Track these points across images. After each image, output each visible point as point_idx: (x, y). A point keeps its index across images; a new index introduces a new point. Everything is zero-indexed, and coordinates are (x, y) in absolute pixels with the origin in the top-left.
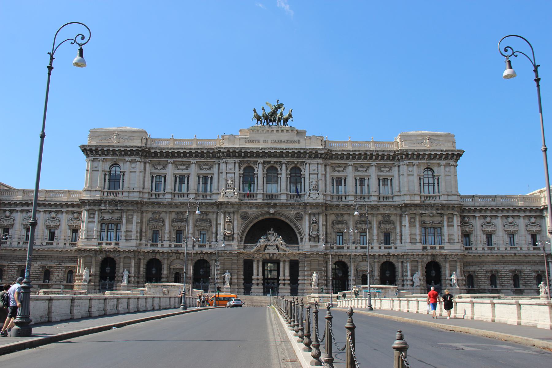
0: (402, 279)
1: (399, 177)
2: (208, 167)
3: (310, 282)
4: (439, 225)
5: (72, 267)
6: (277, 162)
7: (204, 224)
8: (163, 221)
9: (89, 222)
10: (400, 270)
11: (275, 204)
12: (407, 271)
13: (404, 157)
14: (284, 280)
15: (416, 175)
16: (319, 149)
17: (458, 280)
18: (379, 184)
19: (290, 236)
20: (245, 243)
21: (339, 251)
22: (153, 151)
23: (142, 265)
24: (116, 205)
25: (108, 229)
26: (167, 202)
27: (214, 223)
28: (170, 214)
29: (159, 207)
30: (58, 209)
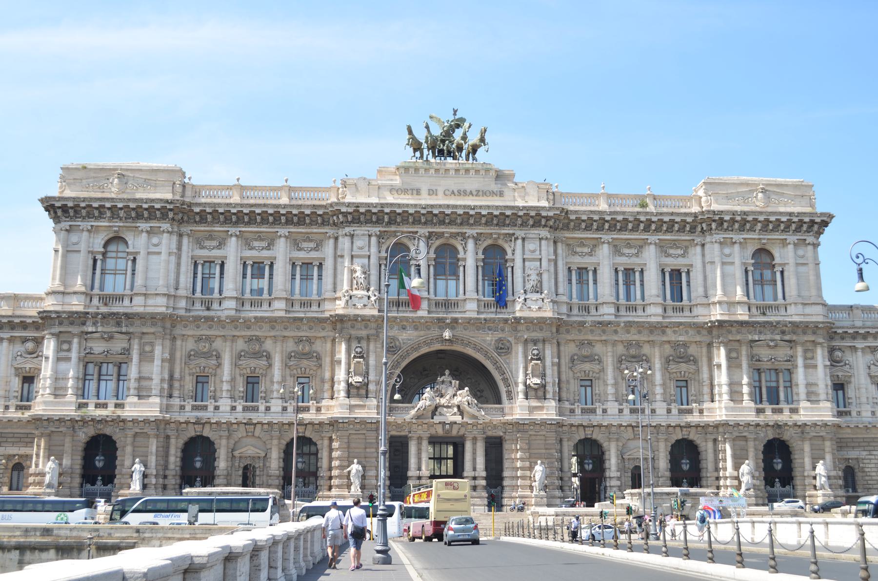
0: (716, 474)
2: (312, 245)
3: (528, 482)
4: (788, 365)
5: (21, 456)
6: (458, 234)
7: (305, 363)
8: (218, 357)
9: (58, 360)
10: (710, 456)
11: (455, 320)
12: (725, 460)
13: (714, 226)
14: (475, 478)
15: (737, 262)
16: (543, 208)
21: (584, 420)
22: (197, 210)
23: (172, 451)
24: (118, 324)
25: (100, 375)
26: (227, 317)
27: (327, 360)
28: (233, 341)
29: (210, 327)
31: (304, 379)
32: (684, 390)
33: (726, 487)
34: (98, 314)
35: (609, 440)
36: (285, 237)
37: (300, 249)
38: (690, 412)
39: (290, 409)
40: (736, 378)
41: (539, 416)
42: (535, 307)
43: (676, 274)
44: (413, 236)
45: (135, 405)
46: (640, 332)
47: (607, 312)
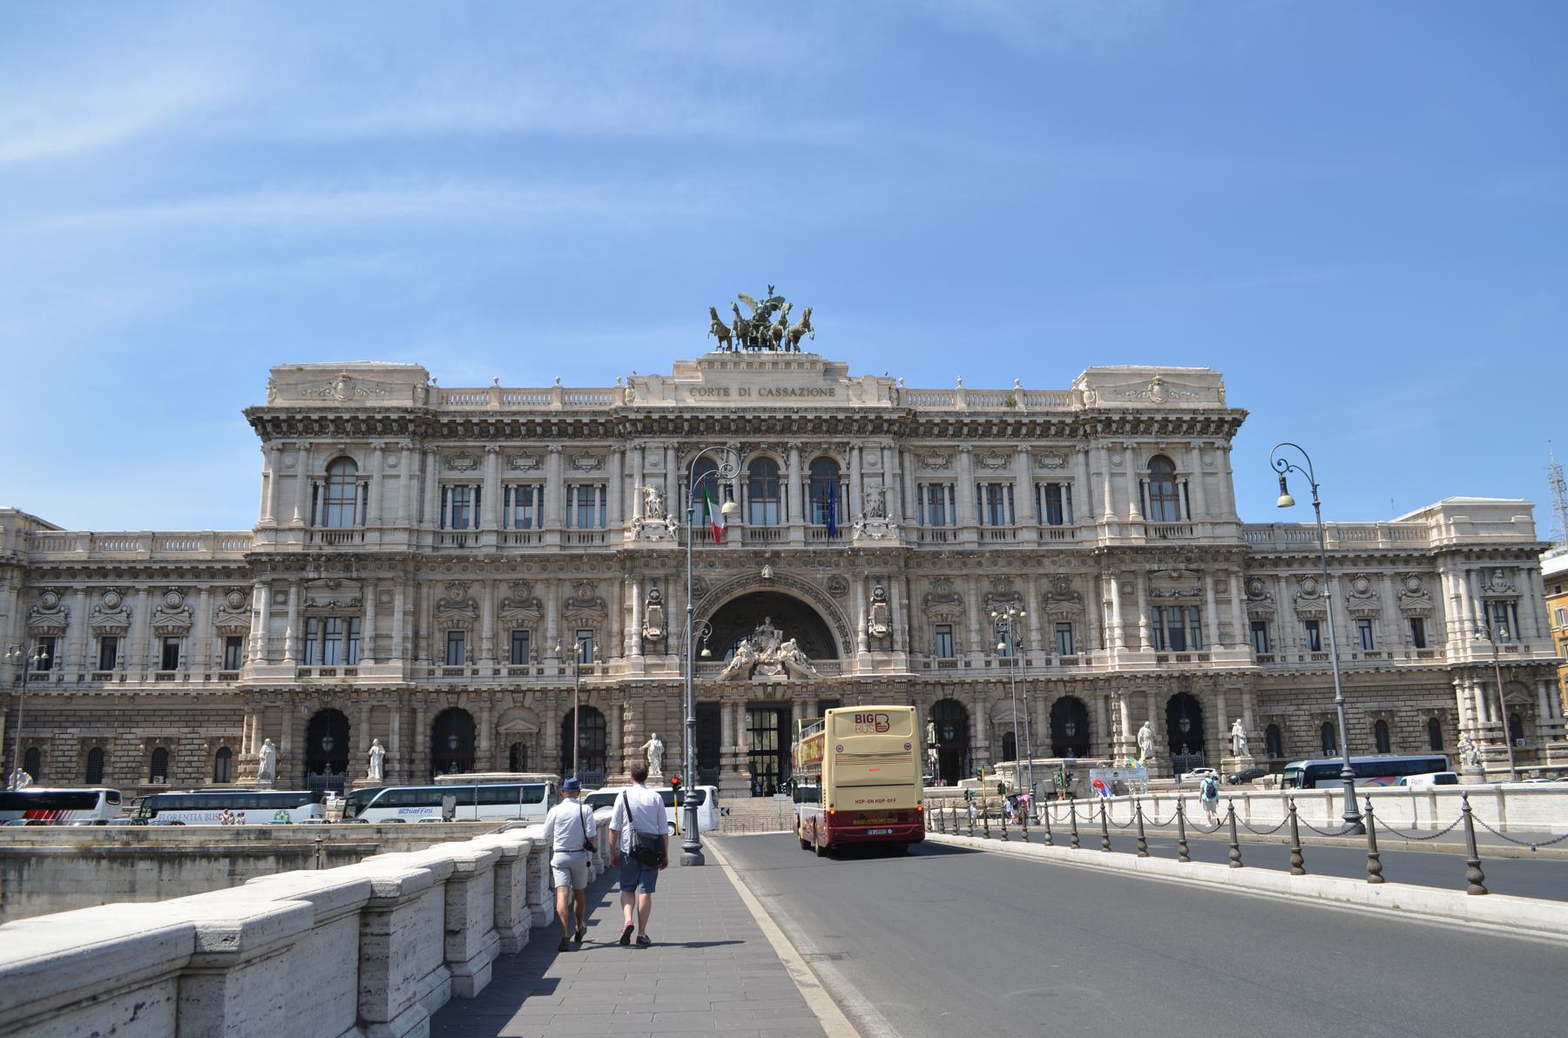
0: (1108, 740)
1: (1089, 480)
2: (593, 462)
4: (1196, 601)
5: (227, 739)
6: (777, 444)
7: (586, 612)
8: (476, 607)
9: (272, 615)
11: (776, 554)
12: (1119, 722)
13: (1099, 427)
15: (1130, 472)
16: (885, 409)
17: (1248, 740)
18: (1038, 499)
19: (818, 638)
21: (943, 676)
22: (445, 420)
23: (420, 728)
24: (347, 568)
25: (325, 633)
26: (486, 556)
29: (465, 570)
30: (187, 582)
31: (586, 633)
32: (1067, 635)
33: (1122, 756)
34: (320, 555)
35: (975, 700)
36: (559, 453)
37: (577, 468)
38: (1075, 662)
39: (569, 671)
40: (1131, 619)
41: (886, 672)
42: (877, 535)
43: (1053, 490)
44: (721, 448)
45: (371, 671)
46: (1010, 564)
47: (968, 540)
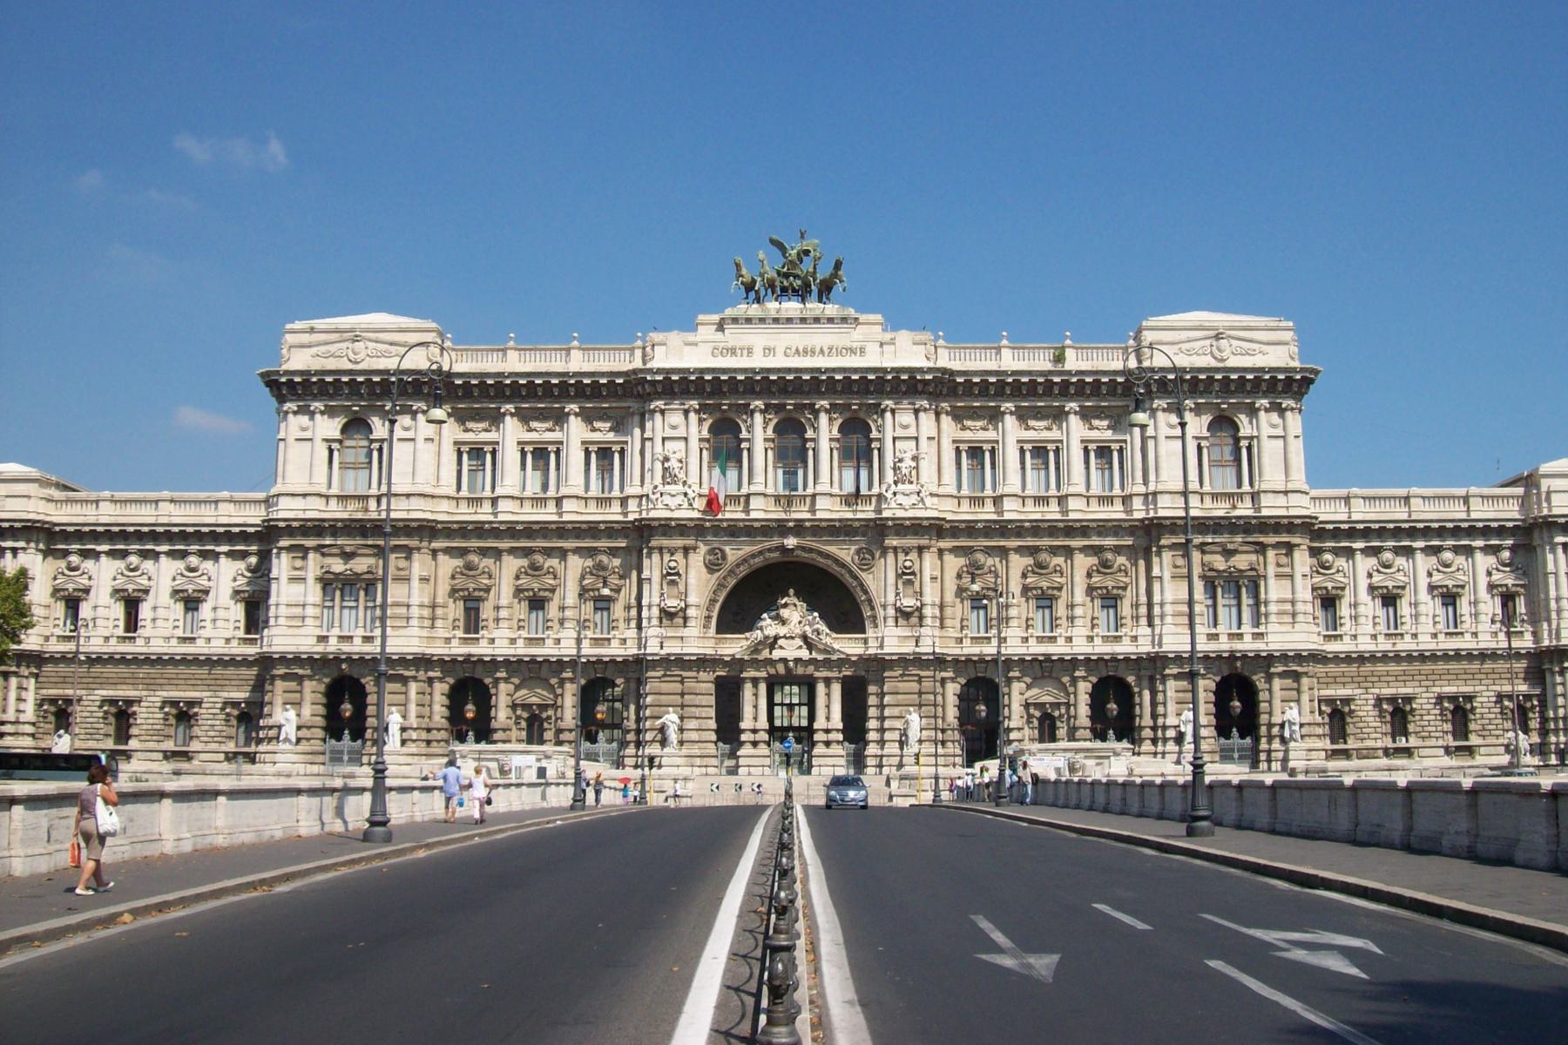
16: (920, 370)
20: (718, 631)
